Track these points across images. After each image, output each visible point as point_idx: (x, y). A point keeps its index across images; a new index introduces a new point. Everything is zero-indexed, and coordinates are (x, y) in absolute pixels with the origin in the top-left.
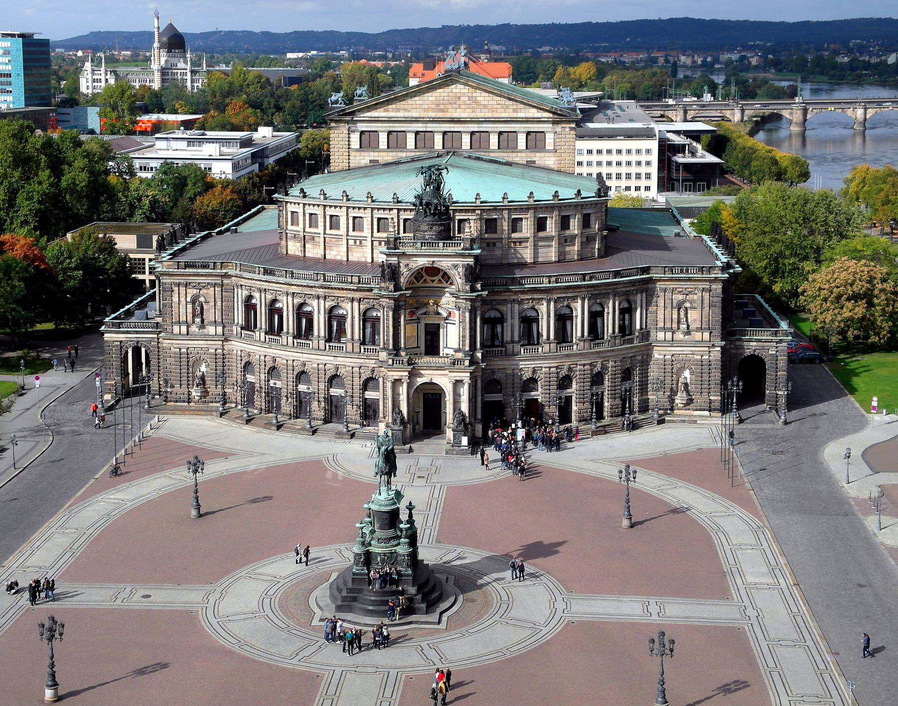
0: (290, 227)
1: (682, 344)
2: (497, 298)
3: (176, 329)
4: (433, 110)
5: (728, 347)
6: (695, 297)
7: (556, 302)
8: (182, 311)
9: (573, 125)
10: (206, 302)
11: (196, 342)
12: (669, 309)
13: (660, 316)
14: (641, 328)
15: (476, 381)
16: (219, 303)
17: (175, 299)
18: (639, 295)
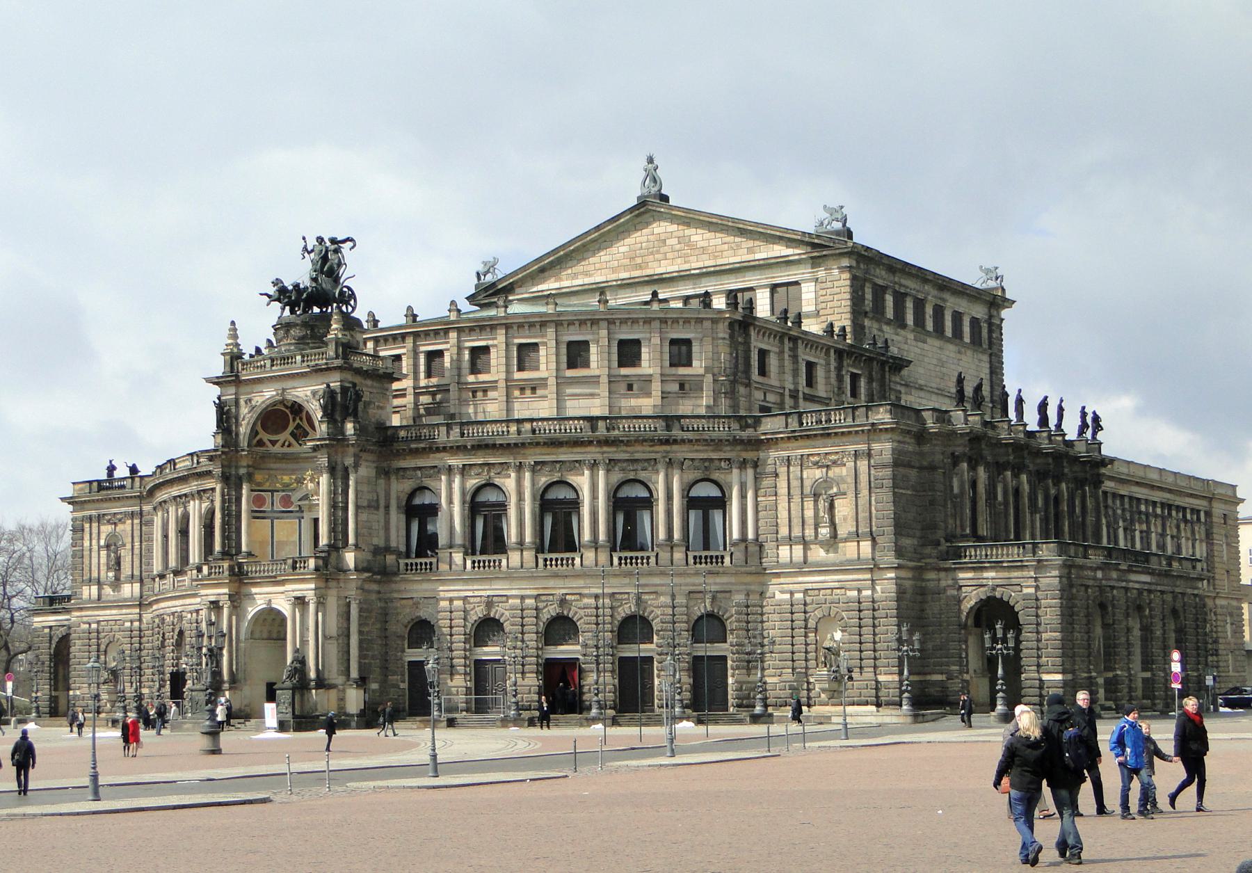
1: (823, 569)
2: (421, 462)
4: (626, 268)
5: (943, 584)
6: (844, 471)
7: (533, 471)
8: (94, 561)
9: (846, 262)
11: (108, 612)
12: (797, 499)
13: (783, 514)
14: (744, 538)
15: (349, 605)
16: (137, 544)
17: (87, 543)
18: (735, 471)
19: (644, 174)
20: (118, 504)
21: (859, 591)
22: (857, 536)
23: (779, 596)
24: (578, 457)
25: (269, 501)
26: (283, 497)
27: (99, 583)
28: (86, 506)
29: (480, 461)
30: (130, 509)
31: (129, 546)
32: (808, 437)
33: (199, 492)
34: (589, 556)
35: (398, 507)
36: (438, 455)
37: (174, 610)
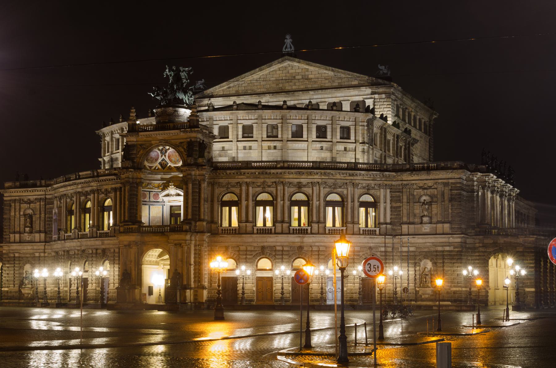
8: (17, 223)
13: (405, 211)
17: (12, 214)
24: (310, 181)
25: (148, 196)
26: (154, 194)
27: (20, 233)
30: (39, 197)
31: (38, 216)
33: (98, 190)
35: (218, 201)
36: (240, 177)
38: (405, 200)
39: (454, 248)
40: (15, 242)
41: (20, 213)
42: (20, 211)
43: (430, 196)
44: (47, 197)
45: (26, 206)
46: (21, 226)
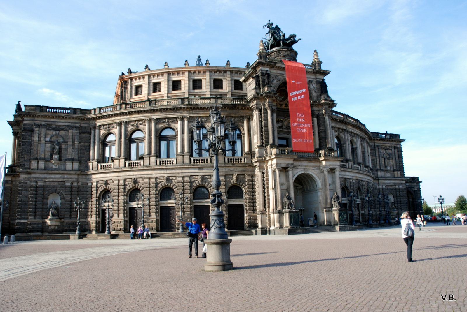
0: (134, 97)
3: (34, 164)
8: (41, 148)
10: (65, 142)
11: (53, 176)
13: (378, 162)
16: (76, 143)
17: (36, 138)
19: (197, 60)
20: (63, 121)
21: (399, 186)
22: (397, 170)
23: (378, 187)
27: (44, 159)
28: (36, 119)
29: (339, 127)
30: (72, 124)
31: (70, 143)
32: (384, 140)
33: (190, 117)
34: (361, 165)
37: (158, 175)
38: (377, 155)
39: (403, 186)
40: (38, 169)
41: (45, 139)
42: (45, 137)
43: (388, 154)
44: (83, 125)
45: (54, 132)
46: (46, 153)
